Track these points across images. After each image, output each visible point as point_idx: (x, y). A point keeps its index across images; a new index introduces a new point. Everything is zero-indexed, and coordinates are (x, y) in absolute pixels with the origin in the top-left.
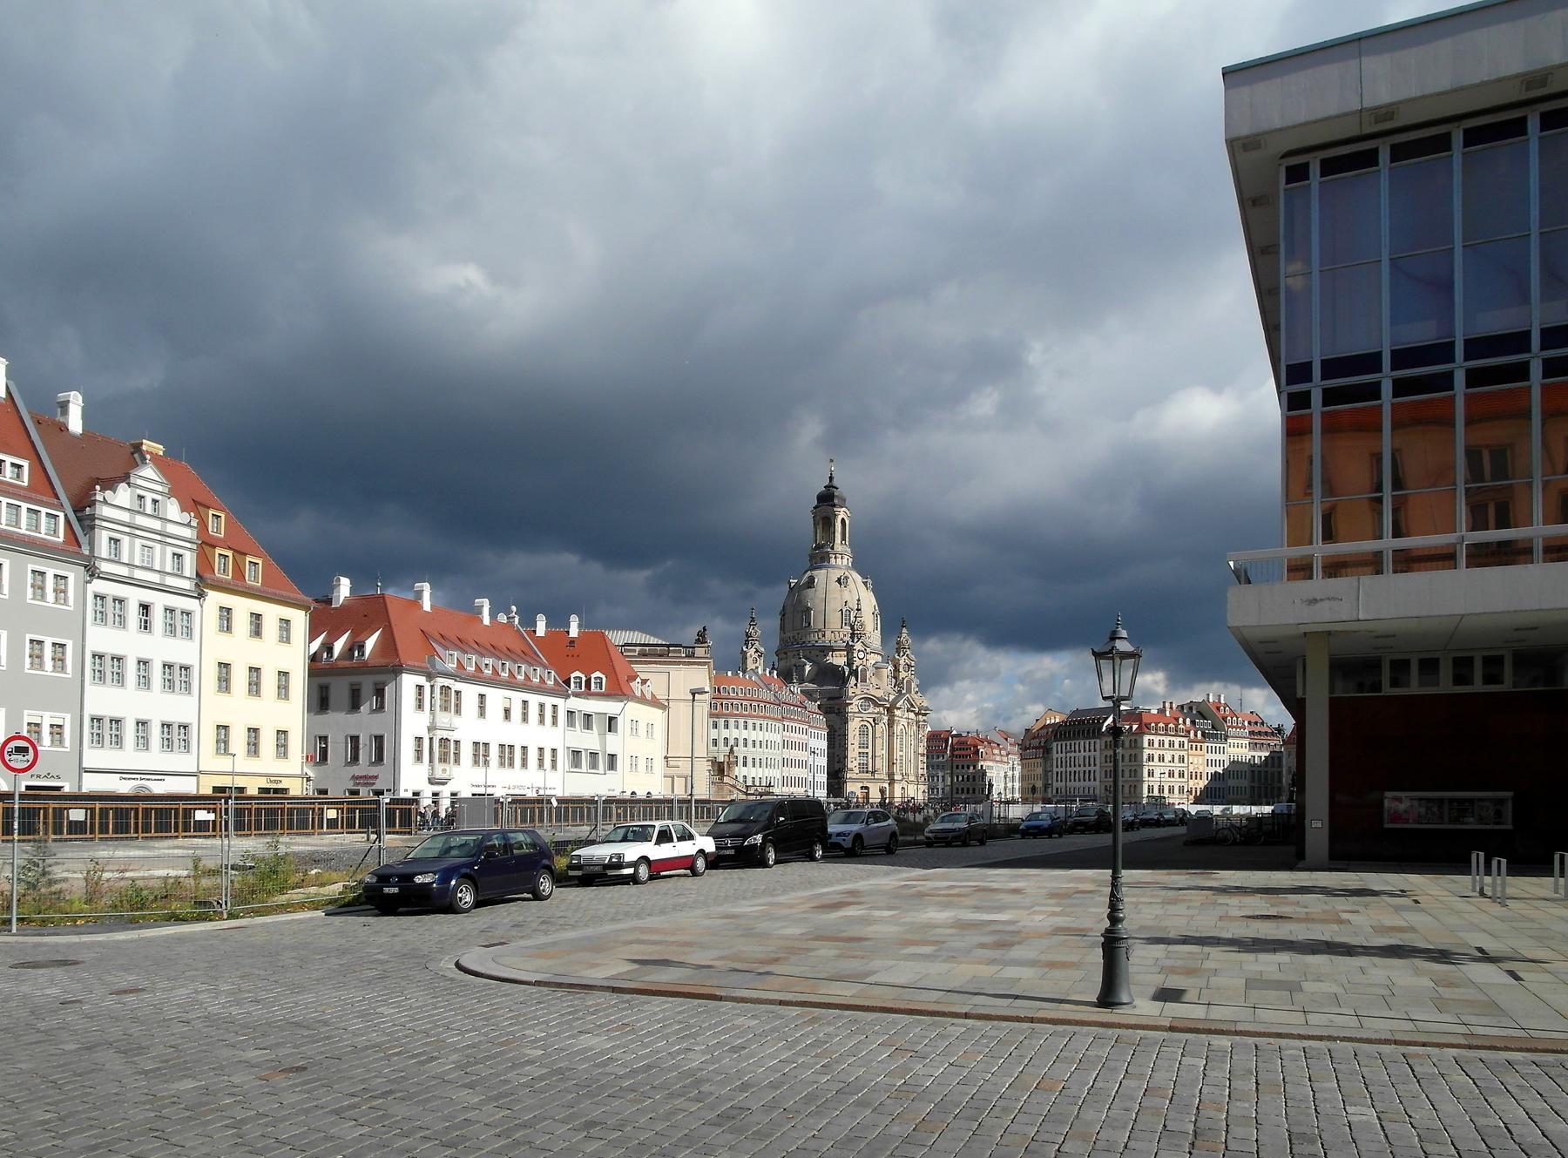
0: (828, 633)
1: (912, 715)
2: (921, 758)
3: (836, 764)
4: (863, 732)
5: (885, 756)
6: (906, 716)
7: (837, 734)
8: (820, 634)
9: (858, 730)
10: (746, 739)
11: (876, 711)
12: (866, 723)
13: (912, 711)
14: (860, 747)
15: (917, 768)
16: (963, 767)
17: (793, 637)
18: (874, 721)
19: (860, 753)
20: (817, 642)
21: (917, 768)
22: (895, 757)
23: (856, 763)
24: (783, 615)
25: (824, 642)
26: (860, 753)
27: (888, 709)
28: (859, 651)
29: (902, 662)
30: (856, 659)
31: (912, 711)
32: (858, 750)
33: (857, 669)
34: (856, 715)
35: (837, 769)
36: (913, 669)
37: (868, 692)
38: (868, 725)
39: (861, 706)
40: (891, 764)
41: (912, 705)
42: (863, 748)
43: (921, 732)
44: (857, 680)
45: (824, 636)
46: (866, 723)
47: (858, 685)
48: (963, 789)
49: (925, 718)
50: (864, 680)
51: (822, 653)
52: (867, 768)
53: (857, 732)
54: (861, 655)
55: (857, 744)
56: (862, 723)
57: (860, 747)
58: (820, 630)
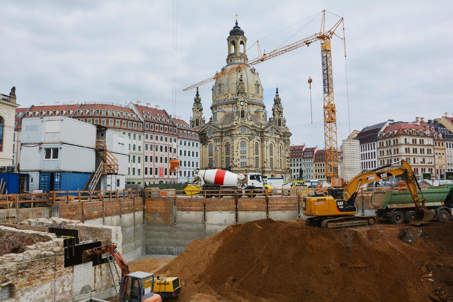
0: (230, 96)
1: (278, 137)
2: (287, 160)
3: (230, 163)
4: (243, 144)
5: (260, 158)
6: (274, 136)
7: (230, 146)
8: (226, 96)
9: (240, 144)
10: (134, 145)
11: (250, 133)
12: (244, 140)
13: (278, 134)
14: (241, 153)
15: (285, 164)
16: (321, 165)
17: (215, 100)
18: (249, 138)
19: (241, 157)
20: (224, 100)
21: (285, 164)
22: (265, 158)
23: (239, 162)
24: (213, 90)
25: (228, 100)
26: (241, 157)
27: (261, 132)
28: (241, 101)
29: (276, 110)
30: (240, 106)
31: (278, 134)
32: (239, 155)
33: (239, 112)
34: (238, 135)
35: (230, 166)
36: (282, 113)
37: (245, 122)
38: (246, 141)
39: (241, 130)
40: (263, 162)
41: (278, 131)
42: (243, 154)
43: (287, 146)
44: (239, 117)
45: (228, 97)
46: (244, 140)
47: (239, 119)
48: (321, 176)
49: (288, 138)
50: (243, 116)
51: (227, 106)
52: (246, 165)
53: (239, 145)
54: (242, 103)
55: (239, 152)
56: (242, 140)
57: (241, 153)
58: (226, 94)
